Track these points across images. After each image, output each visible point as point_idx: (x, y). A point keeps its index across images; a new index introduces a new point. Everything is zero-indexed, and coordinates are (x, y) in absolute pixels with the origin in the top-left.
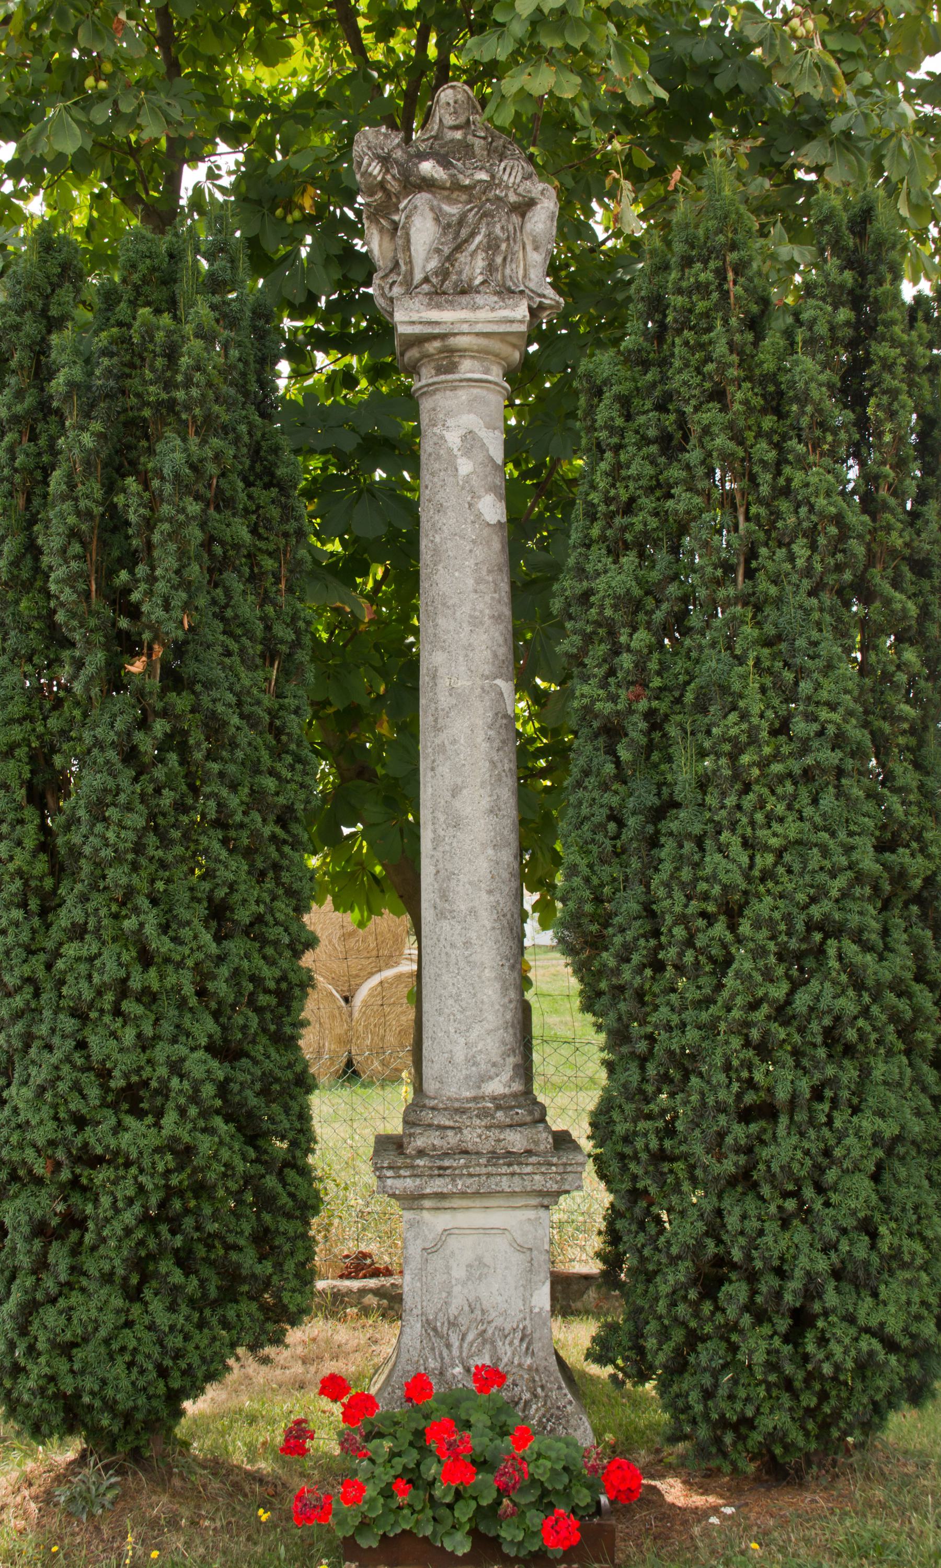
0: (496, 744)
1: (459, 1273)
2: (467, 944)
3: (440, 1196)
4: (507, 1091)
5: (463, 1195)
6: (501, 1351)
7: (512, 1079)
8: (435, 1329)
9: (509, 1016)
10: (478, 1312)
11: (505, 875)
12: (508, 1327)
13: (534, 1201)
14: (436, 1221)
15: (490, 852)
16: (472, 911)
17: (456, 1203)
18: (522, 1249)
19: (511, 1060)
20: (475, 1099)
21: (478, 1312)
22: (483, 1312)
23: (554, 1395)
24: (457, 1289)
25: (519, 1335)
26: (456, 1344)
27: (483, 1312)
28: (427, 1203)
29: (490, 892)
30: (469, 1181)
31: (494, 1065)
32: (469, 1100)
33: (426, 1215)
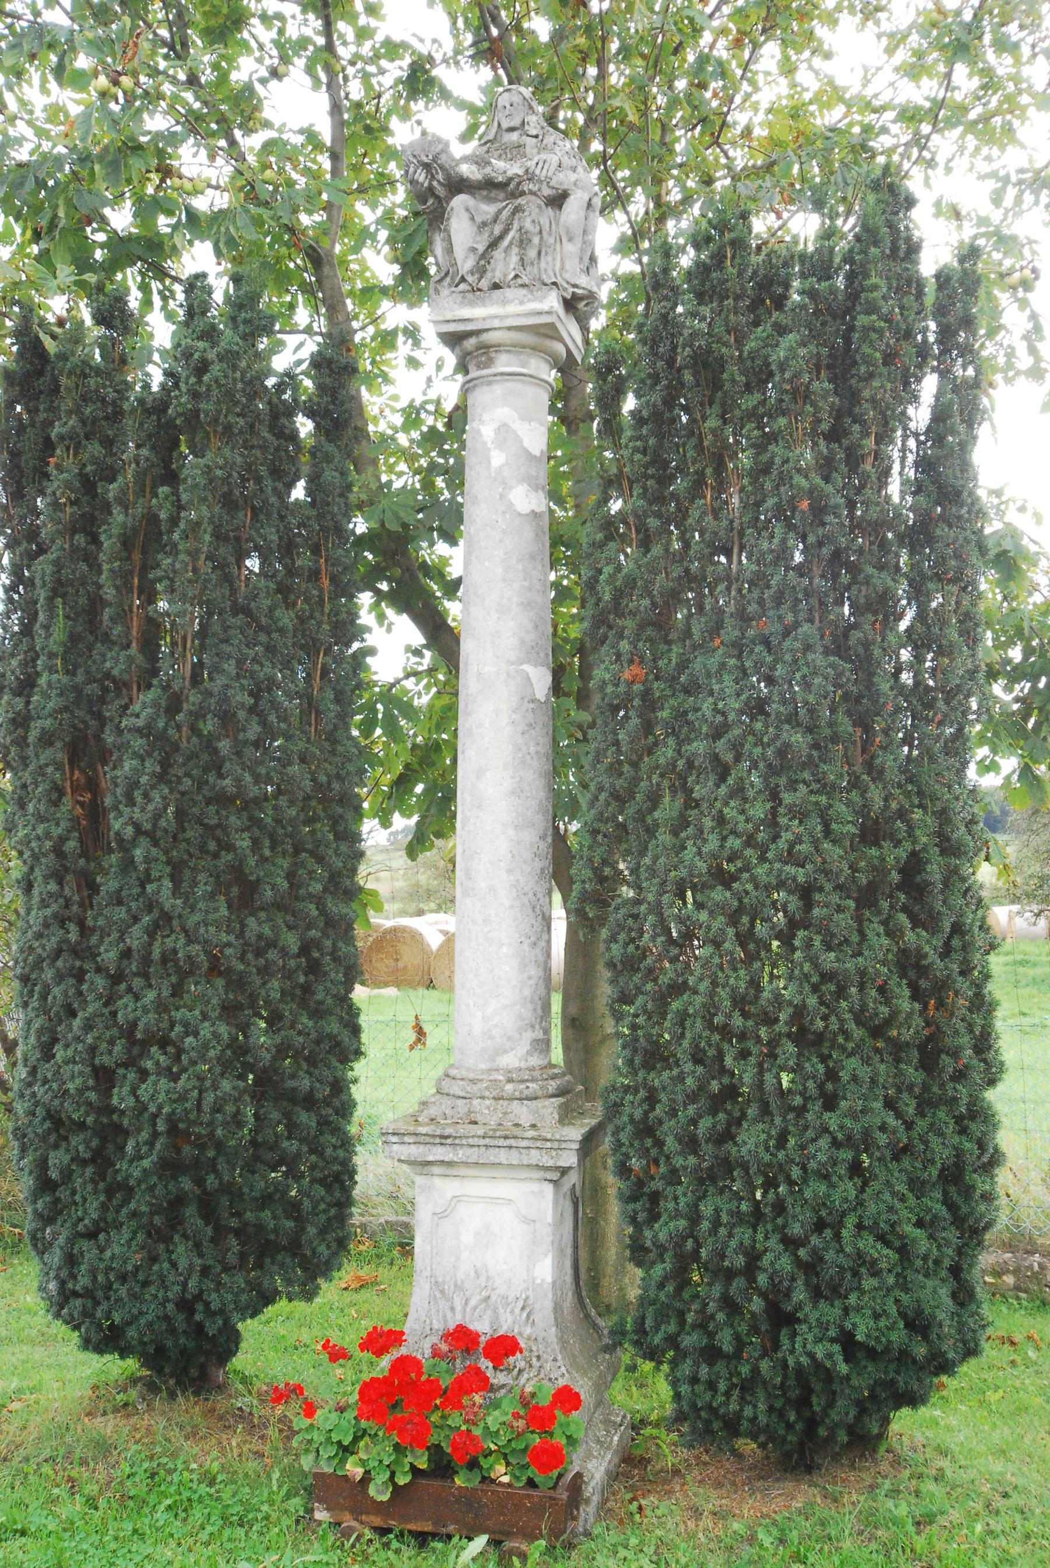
0: (522, 727)
1: (467, 1239)
2: (486, 921)
3: (450, 1164)
4: (523, 1065)
5: (466, 1164)
6: (502, 1319)
7: (529, 1053)
8: (442, 1292)
9: (527, 992)
10: (483, 1279)
11: (528, 855)
12: (512, 1296)
13: (540, 1174)
14: (446, 1188)
15: (511, 832)
16: (492, 889)
17: (463, 1171)
18: (527, 1220)
19: (529, 1035)
20: (489, 1071)
21: (483, 1279)
22: (488, 1278)
23: (548, 1366)
24: (465, 1255)
25: (520, 1303)
26: (459, 1308)
27: (488, 1278)
28: (436, 1170)
29: (510, 871)
30: (469, 1151)
31: (509, 1038)
32: (483, 1072)
33: (437, 1181)
